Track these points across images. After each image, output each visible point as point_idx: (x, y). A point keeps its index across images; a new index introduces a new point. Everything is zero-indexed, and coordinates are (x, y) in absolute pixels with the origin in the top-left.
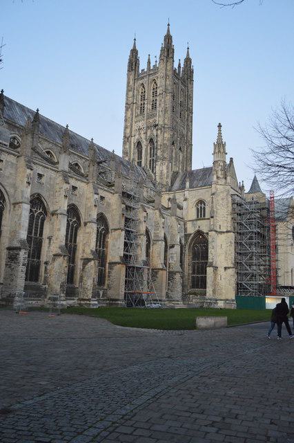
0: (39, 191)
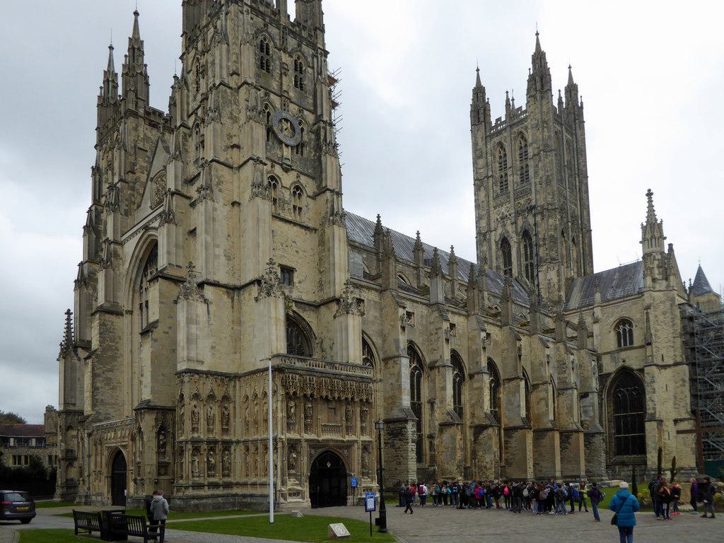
0: (411, 338)
